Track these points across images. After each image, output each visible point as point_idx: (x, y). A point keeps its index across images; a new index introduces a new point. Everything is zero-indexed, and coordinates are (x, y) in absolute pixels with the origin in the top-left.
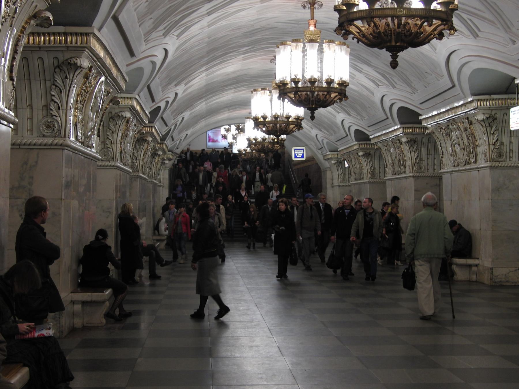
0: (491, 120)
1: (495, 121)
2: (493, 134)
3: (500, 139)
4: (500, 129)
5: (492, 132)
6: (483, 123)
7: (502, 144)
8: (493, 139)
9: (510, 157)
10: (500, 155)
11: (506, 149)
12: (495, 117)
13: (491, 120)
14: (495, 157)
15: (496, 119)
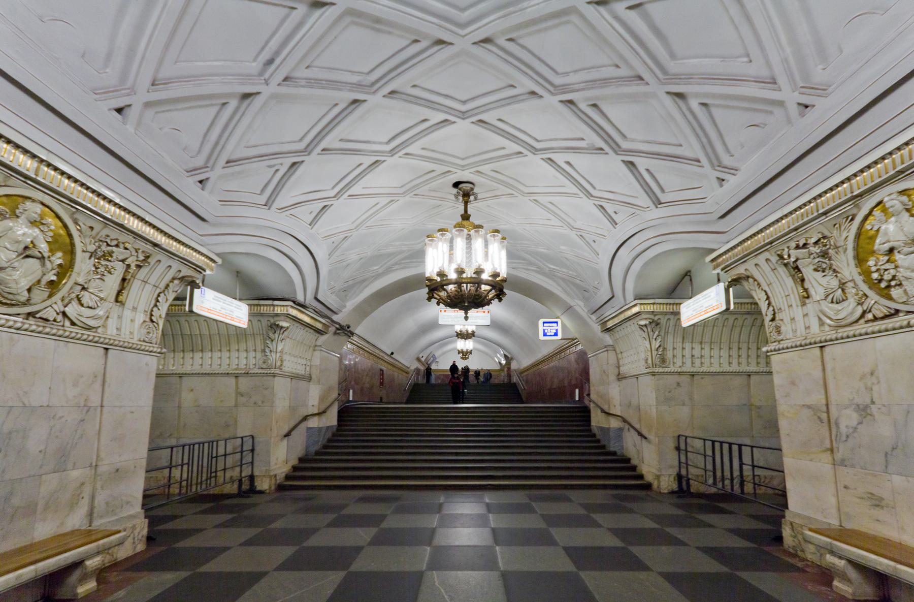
0: (653, 325)
1: (658, 326)
2: (655, 339)
3: (662, 345)
4: (663, 335)
5: (655, 337)
6: (645, 329)
7: (664, 349)
8: (655, 345)
9: (674, 363)
10: (663, 361)
11: (669, 354)
12: (659, 321)
13: (653, 325)
14: (658, 363)
15: (658, 324)
